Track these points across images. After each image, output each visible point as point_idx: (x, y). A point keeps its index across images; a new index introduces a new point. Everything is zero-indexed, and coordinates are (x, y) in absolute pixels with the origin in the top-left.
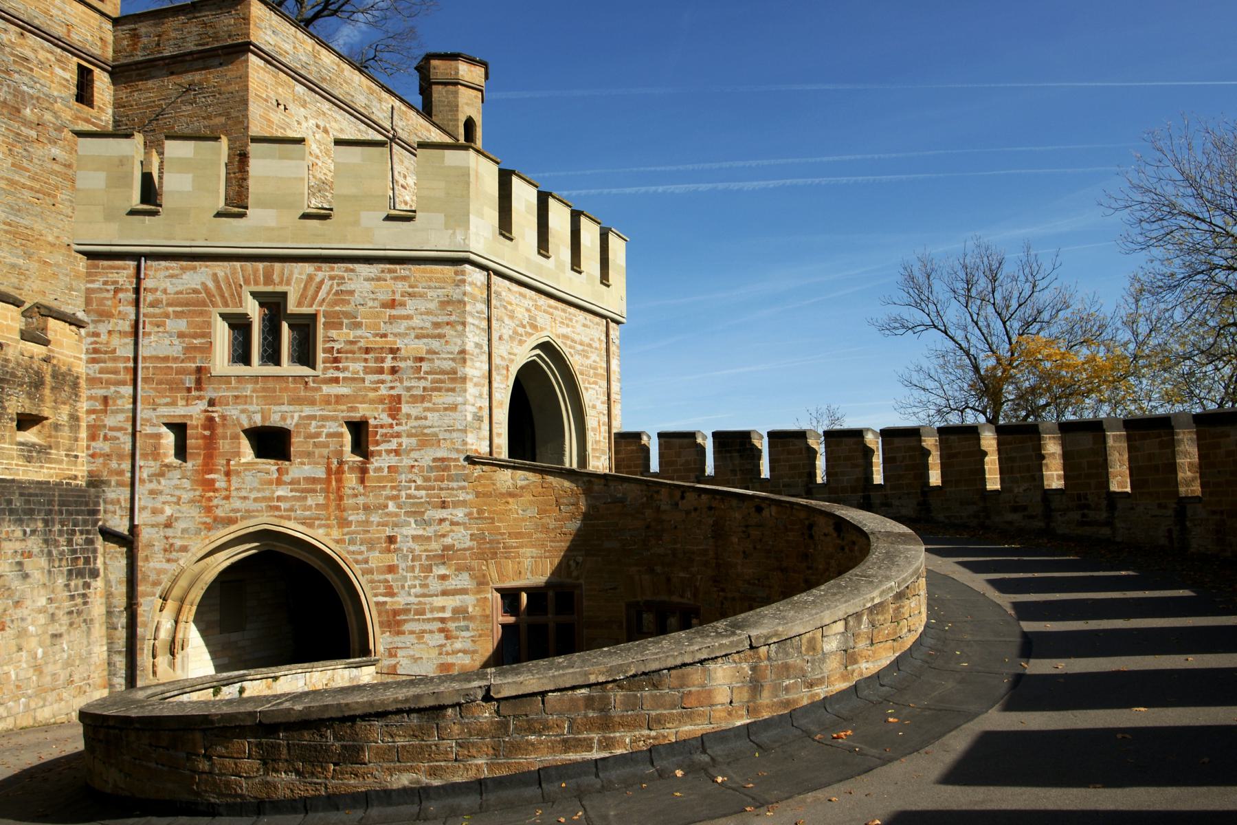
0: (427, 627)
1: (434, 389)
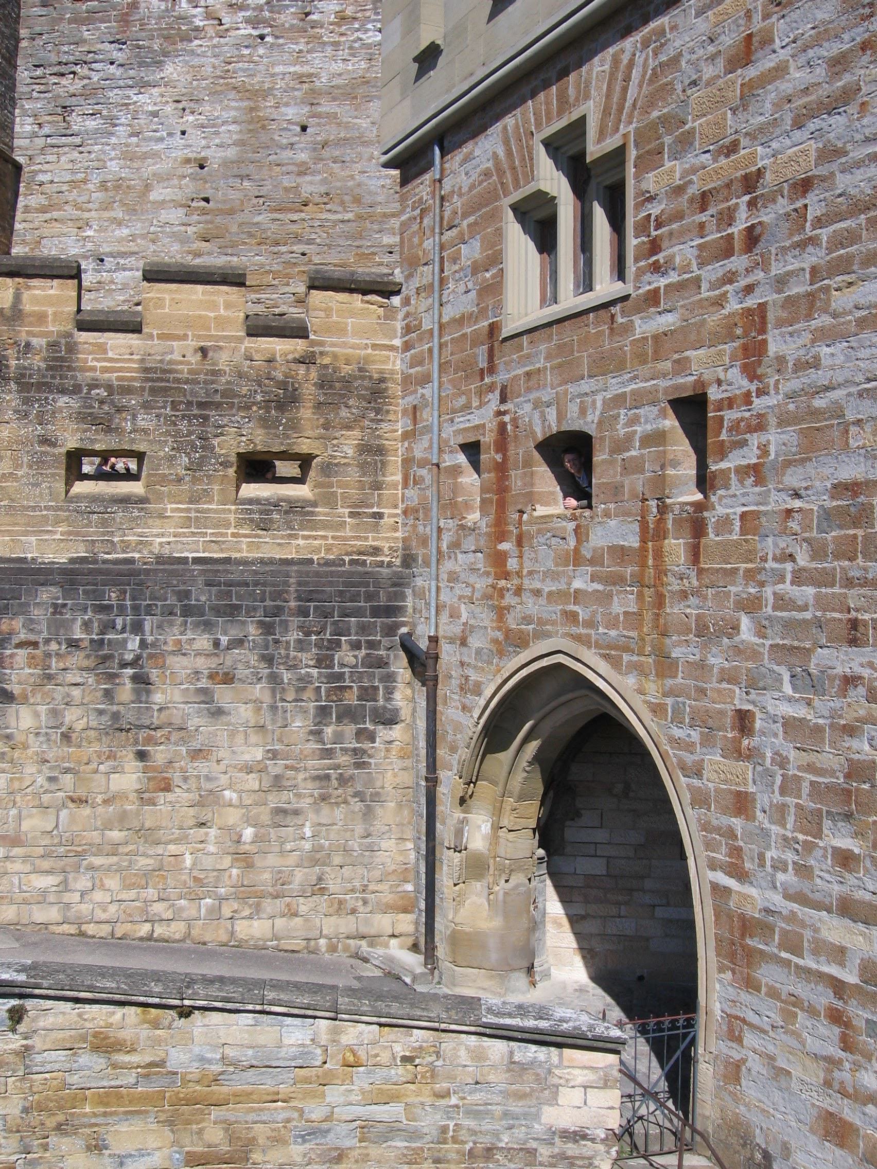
0: (803, 990)
1: (842, 266)
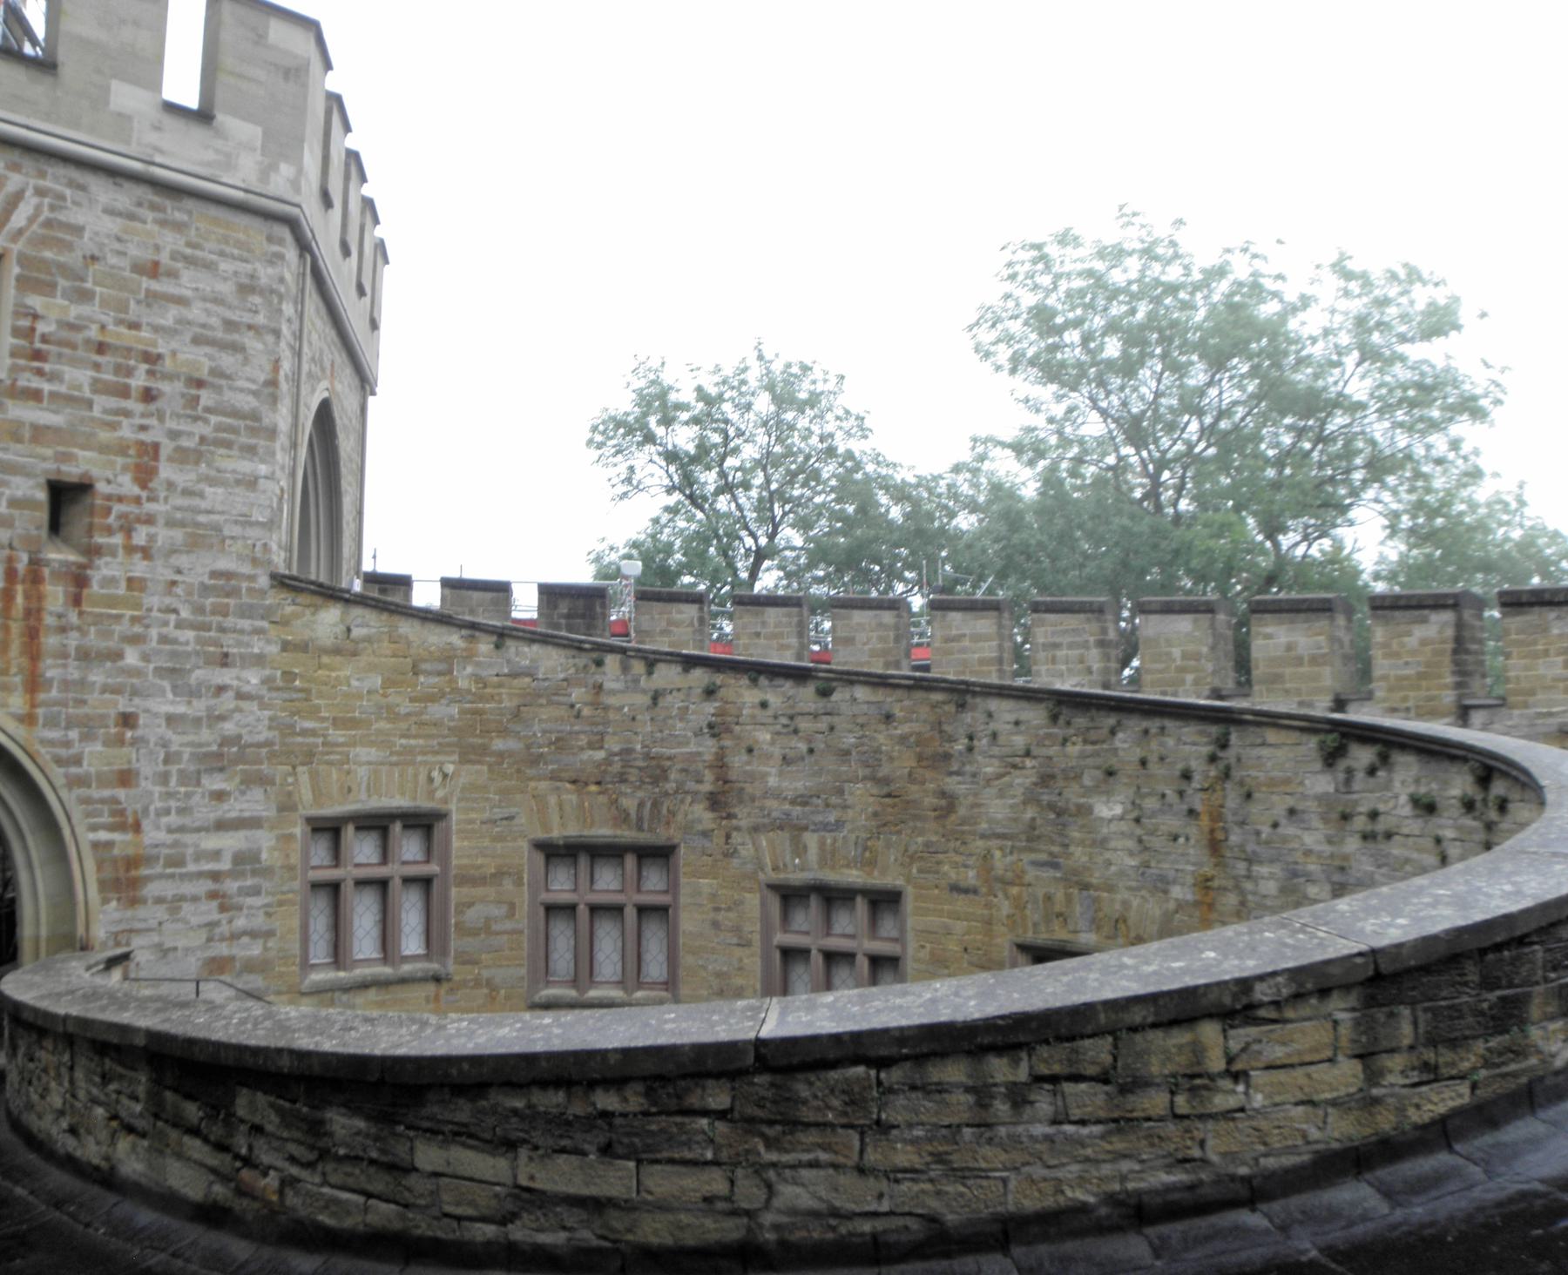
0: (188, 888)
